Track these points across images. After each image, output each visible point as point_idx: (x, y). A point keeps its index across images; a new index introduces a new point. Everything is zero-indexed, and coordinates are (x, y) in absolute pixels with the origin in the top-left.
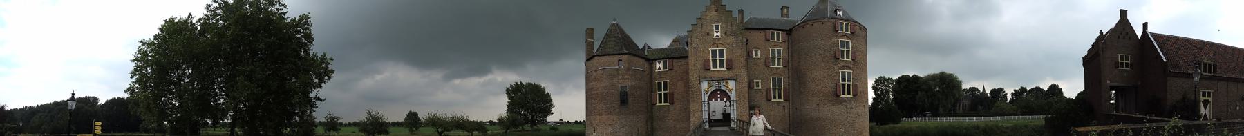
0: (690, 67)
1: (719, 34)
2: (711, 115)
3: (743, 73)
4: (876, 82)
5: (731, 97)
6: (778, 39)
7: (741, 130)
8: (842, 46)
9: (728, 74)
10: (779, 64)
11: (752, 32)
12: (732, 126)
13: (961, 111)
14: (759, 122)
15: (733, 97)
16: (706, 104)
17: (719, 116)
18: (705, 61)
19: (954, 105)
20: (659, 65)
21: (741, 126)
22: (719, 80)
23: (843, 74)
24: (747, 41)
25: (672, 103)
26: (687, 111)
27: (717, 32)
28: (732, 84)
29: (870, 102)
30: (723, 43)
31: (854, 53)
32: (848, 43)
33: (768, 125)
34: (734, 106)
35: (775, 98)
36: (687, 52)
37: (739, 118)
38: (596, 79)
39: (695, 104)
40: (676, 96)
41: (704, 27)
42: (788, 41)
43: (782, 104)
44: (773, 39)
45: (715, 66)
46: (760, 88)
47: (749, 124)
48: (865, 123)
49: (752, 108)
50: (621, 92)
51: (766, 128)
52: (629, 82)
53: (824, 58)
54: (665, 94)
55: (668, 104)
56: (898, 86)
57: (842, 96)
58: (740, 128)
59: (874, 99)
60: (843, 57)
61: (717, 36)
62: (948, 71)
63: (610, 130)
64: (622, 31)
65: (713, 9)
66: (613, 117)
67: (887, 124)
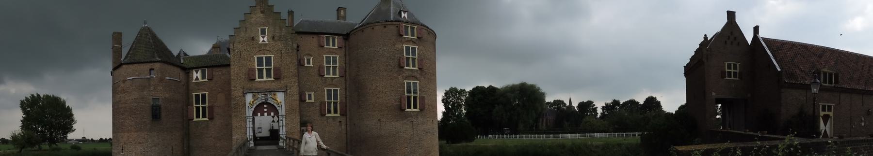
1: (266, 39)
2: (256, 132)
3: (293, 83)
4: (447, 93)
5: (280, 114)
6: (334, 45)
7: (291, 150)
8: (408, 53)
9: (275, 85)
10: (334, 73)
11: (303, 36)
12: (281, 144)
13: (544, 127)
14: (312, 140)
15: (282, 111)
16: (251, 120)
17: (265, 133)
18: (249, 70)
20: (197, 75)
21: (291, 145)
22: (265, 93)
23: (409, 84)
24: (298, 47)
25: (211, 118)
26: (228, 130)
28: (280, 97)
29: (440, 116)
31: (421, 60)
32: (414, 49)
33: (321, 143)
34: (283, 122)
35: (329, 112)
36: (229, 59)
38: (124, 91)
42: (345, 47)
43: (339, 120)
44: (328, 44)
45: (261, 76)
46: (313, 100)
47: (300, 142)
48: (433, 142)
50: (153, 106)
51: (319, 147)
52: (161, 94)
54: (204, 108)
55: (206, 119)
57: (407, 110)
58: (290, 146)
59: (444, 113)
60: (408, 65)
61: (263, 41)
62: (530, 82)
64: (154, 36)
65: (259, 11)
66: (143, 134)
67: (458, 143)
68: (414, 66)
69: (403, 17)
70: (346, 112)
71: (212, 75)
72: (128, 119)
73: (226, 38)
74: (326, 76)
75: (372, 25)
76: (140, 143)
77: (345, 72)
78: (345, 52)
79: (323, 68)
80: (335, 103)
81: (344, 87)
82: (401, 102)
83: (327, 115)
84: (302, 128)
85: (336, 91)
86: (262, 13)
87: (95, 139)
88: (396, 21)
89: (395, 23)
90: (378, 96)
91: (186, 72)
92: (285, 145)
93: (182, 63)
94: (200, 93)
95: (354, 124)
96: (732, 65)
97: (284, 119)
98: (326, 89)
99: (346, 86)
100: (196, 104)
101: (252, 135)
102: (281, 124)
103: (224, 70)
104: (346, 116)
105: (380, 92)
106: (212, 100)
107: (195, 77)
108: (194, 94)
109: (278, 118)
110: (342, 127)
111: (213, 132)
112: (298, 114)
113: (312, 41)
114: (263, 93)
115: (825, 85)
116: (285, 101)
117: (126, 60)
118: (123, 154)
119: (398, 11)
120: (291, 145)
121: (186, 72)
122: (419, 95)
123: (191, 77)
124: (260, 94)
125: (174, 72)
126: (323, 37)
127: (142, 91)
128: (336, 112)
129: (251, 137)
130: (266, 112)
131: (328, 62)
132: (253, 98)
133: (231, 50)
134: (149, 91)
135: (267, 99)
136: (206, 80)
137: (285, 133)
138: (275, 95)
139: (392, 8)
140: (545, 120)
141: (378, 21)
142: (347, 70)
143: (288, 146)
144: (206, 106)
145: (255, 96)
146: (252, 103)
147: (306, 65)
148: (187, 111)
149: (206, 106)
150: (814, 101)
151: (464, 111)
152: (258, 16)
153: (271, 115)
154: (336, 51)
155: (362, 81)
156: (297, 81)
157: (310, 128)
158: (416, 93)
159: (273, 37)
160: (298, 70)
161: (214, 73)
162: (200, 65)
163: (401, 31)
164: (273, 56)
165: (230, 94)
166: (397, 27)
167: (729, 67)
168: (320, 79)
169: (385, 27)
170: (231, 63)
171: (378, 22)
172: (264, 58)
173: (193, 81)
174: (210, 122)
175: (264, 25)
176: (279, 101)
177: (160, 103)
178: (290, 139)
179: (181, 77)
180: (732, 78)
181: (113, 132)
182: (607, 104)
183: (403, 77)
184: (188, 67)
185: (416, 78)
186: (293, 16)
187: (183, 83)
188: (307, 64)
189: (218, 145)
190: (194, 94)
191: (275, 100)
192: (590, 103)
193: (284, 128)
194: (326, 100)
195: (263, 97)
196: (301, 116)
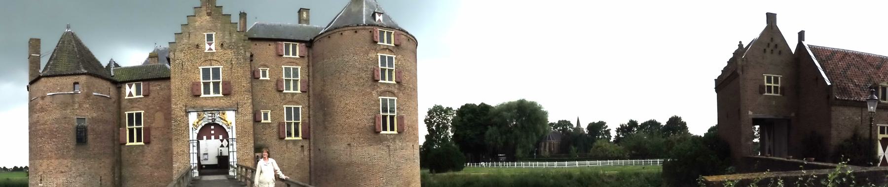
0: (173, 93)
1: (213, 47)
2: (201, 159)
4: (430, 113)
5: (230, 137)
6: (294, 54)
7: (243, 180)
8: (383, 64)
9: (224, 102)
10: (295, 88)
11: (258, 43)
13: (547, 153)
15: (232, 134)
16: (195, 144)
17: (212, 160)
18: (193, 84)
19: (538, 145)
20: (130, 90)
21: (244, 174)
22: (212, 111)
24: (252, 56)
25: (147, 142)
26: (167, 155)
27: (210, 44)
29: (422, 141)
30: (219, 59)
31: (398, 73)
32: (390, 59)
35: (289, 134)
36: (169, 71)
37: (240, 164)
38: (42, 110)
39: (180, 144)
40: (153, 133)
41: (192, 36)
43: (300, 144)
44: (287, 53)
45: (207, 91)
46: (269, 121)
47: (254, 171)
48: (414, 170)
49: (258, 149)
50: (77, 128)
51: (277, 177)
52: (88, 113)
53: (359, 79)
54: (139, 130)
56: (460, 118)
58: (242, 176)
59: (427, 137)
60: (383, 78)
61: (210, 49)
62: (529, 99)
63: (61, 179)
64: (79, 43)
65: (205, 13)
67: (444, 171)
68: (390, 79)
69: (377, 20)
70: (309, 135)
71: (149, 90)
72: (48, 143)
73: (164, 45)
74: (285, 91)
75: (341, 29)
76: (62, 172)
77: (309, 86)
78: (309, 62)
79: (282, 82)
80: (296, 124)
81: (307, 104)
82: (375, 123)
83: (287, 138)
84: (257, 154)
85: (297, 110)
86: (208, 15)
87: (8, 167)
88: (369, 25)
89: (367, 27)
90: (348, 115)
91: (118, 86)
92: (235, 175)
93: (113, 76)
94: (134, 112)
95: (319, 150)
96: (772, 78)
97: (235, 143)
98: (285, 106)
99: (309, 104)
100: (129, 125)
101: (197, 162)
102: (231, 150)
103: (163, 84)
104: (309, 139)
105: (350, 110)
106: (149, 121)
107: (127, 93)
108: (127, 113)
109: (228, 142)
110: (305, 152)
111: (150, 159)
112: (251, 138)
113: (270, 48)
114: (209, 112)
115: (884, 102)
116: (236, 122)
117: (45, 72)
118: (42, 185)
119: (372, 13)
120: (244, 174)
121: (118, 86)
122: (397, 114)
123: (123, 92)
124: (206, 113)
125: (103, 86)
126: (282, 45)
127: (65, 110)
128: (297, 134)
129: (195, 165)
130: (213, 134)
131: (288, 74)
132: (198, 118)
133: (171, 59)
134: (73, 109)
135: (215, 119)
136: (141, 96)
137: (236, 160)
138: (224, 114)
139: (364, 9)
140: (548, 145)
141: (347, 25)
142: (311, 84)
143: (239, 176)
144: (141, 128)
145: (199, 115)
146: (196, 124)
147: (261, 78)
148: (119, 134)
149: (141, 128)
150: (871, 121)
151: (451, 134)
152: (204, 19)
153: (219, 138)
154: (298, 62)
155: (329, 97)
156: (251, 97)
157: (265, 154)
158: (394, 112)
159: (222, 44)
160: (252, 85)
161: (151, 88)
162: (134, 78)
163: (375, 38)
164: (222, 67)
165: (170, 114)
166: (371, 32)
167: (769, 81)
168: (278, 95)
169: (356, 32)
170: (172, 76)
171: (348, 26)
172: (211, 69)
173: (126, 97)
174: (146, 147)
175: (211, 30)
176: (229, 122)
177: (86, 124)
178: (242, 168)
179: (111, 93)
180: (773, 94)
181: (30, 159)
182: (622, 126)
183: (377, 92)
184: (119, 81)
185: (393, 94)
186: (245, 19)
187: (114, 100)
188: (263, 77)
189: (156, 174)
190: (127, 113)
191: (225, 120)
192: (601, 124)
193: (235, 153)
194: (285, 121)
195: (209, 116)
196: (255, 140)
